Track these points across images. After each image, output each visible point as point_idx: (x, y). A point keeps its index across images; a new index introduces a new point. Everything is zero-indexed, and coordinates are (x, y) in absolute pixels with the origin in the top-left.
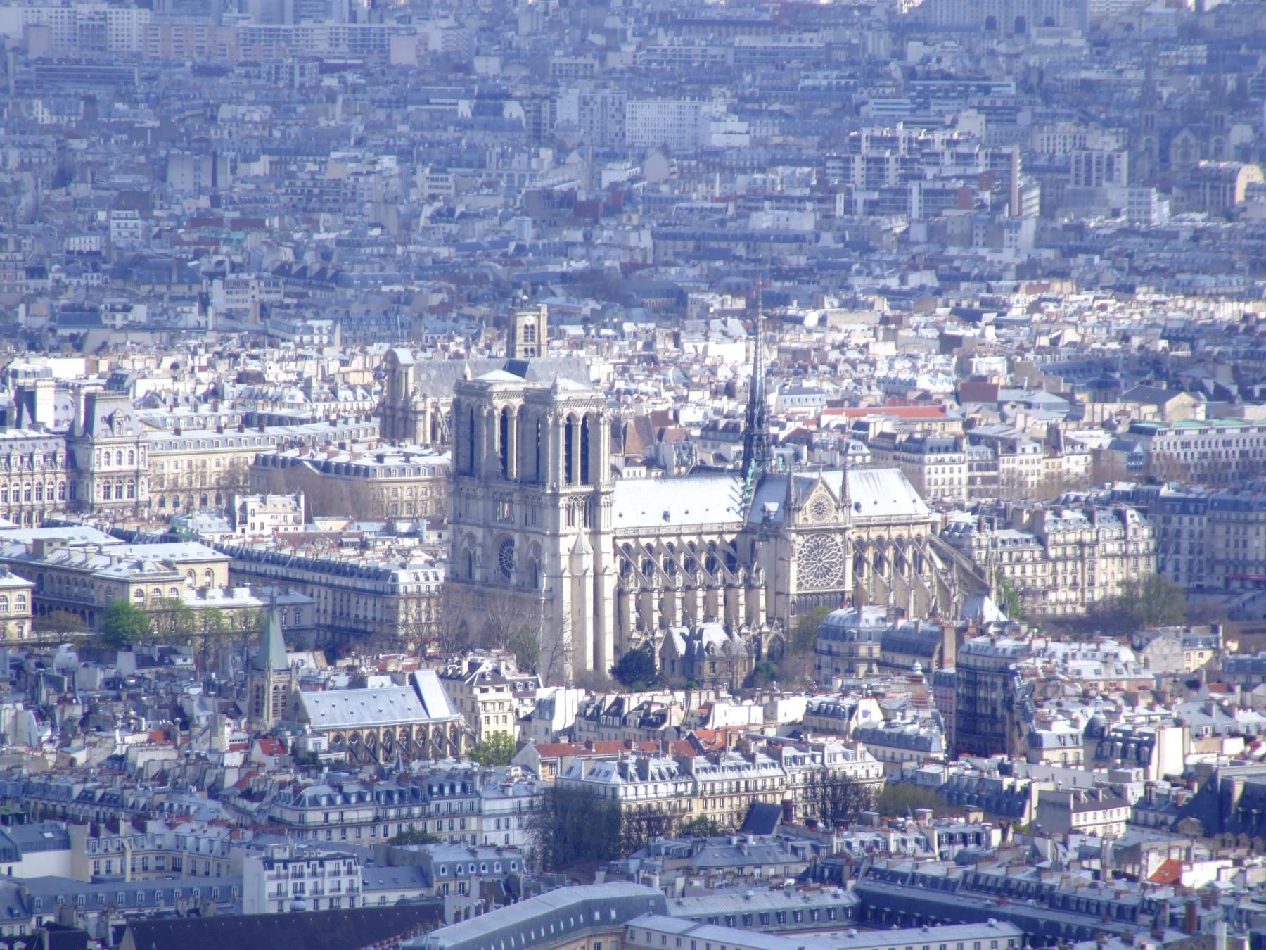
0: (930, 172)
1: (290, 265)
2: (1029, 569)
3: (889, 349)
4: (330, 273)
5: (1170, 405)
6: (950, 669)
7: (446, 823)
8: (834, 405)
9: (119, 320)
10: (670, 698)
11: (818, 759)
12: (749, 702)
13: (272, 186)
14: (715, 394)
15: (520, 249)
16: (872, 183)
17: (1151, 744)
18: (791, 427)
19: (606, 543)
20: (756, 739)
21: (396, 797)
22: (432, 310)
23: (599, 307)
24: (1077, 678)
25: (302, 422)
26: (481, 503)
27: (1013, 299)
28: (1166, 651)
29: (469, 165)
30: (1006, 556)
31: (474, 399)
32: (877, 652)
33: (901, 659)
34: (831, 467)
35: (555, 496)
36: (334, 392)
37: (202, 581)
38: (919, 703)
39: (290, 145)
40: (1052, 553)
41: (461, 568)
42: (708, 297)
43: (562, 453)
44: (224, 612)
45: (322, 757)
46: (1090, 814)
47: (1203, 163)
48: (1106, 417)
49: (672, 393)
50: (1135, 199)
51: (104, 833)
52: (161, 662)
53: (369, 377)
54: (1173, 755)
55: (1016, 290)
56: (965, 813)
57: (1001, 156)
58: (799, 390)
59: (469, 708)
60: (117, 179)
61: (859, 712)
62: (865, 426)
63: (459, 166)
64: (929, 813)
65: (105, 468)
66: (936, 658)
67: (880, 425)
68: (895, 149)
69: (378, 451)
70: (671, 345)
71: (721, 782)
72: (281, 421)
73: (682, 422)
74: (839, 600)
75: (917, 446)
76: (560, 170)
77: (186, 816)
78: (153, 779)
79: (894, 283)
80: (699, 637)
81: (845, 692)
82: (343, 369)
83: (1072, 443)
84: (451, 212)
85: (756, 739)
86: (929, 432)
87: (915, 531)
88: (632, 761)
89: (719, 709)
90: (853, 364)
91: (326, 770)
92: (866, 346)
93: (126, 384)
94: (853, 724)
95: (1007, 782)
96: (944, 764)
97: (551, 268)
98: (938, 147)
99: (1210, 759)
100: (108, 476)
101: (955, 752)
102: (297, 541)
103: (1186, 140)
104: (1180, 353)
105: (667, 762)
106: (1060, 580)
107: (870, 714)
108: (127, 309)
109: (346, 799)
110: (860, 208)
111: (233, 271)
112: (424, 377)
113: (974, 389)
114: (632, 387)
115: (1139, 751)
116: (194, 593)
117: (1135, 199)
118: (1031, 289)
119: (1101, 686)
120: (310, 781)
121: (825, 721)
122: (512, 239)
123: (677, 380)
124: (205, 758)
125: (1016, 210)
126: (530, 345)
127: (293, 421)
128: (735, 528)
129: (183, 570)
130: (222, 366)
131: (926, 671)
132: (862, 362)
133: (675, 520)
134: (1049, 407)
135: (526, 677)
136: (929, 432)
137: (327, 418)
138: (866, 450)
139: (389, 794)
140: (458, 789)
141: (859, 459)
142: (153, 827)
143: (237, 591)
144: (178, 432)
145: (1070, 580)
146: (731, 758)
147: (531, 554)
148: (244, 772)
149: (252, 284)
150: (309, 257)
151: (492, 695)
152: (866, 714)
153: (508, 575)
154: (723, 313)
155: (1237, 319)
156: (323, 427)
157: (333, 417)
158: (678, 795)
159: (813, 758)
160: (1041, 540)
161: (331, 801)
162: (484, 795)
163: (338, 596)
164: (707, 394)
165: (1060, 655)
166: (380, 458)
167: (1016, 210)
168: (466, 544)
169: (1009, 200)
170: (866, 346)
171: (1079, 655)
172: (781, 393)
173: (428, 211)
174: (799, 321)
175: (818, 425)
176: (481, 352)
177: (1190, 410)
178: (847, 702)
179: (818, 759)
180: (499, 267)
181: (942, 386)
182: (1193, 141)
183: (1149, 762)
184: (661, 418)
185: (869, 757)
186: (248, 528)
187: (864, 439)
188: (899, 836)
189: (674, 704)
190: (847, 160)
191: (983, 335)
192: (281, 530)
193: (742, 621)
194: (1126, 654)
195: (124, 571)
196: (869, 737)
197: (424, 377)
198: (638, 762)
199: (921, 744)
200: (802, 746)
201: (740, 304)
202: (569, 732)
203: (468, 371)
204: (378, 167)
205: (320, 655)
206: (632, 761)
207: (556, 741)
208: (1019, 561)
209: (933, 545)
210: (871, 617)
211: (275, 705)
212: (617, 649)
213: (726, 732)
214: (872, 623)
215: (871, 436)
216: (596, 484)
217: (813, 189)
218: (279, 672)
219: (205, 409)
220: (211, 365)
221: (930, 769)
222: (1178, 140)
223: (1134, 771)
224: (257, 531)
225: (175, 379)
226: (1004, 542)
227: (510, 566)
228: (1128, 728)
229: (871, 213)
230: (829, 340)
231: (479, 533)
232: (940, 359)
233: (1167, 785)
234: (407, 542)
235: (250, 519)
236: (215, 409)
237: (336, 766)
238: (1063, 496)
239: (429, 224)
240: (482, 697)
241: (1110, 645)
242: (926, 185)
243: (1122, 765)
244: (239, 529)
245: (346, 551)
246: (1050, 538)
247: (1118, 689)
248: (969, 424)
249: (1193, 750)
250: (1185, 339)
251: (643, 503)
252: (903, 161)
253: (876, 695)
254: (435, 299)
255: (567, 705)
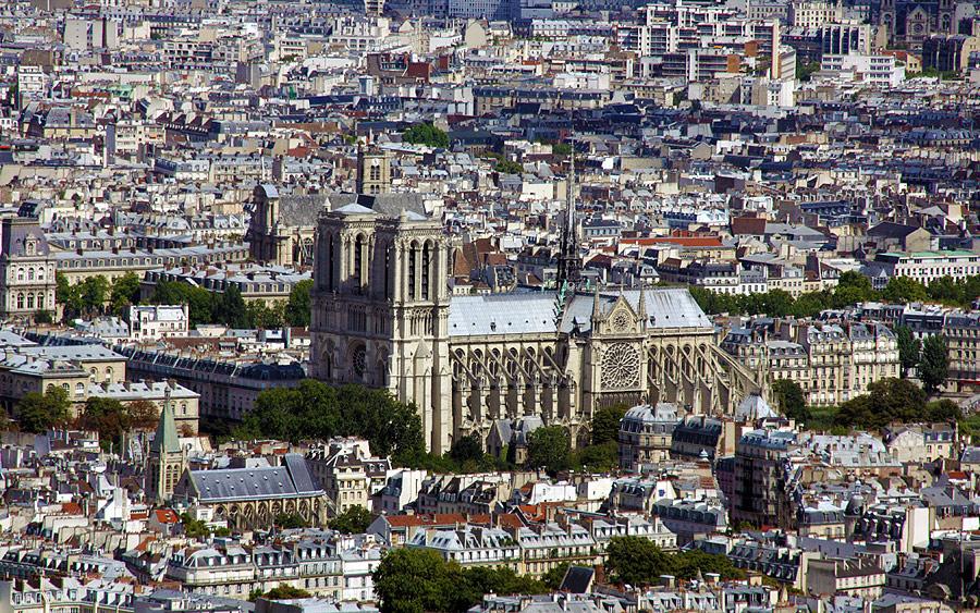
0: (705, 40)
1: (171, 114)
2: (794, 373)
3: (673, 189)
4: (205, 120)
5: (909, 238)
6: (730, 455)
7: (312, 581)
8: (628, 236)
9: (28, 157)
10: (498, 479)
11: (623, 531)
12: (565, 482)
13: (153, 47)
14: (529, 225)
15: (364, 102)
16: (658, 46)
17: (902, 521)
18: (593, 253)
19: (443, 348)
20: (571, 513)
21: (271, 559)
22: (291, 152)
23: (430, 152)
24: (839, 465)
25: (185, 245)
26: (338, 314)
27: (776, 148)
28: (911, 443)
29: (318, 31)
30: (774, 362)
31: (333, 228)
32: (669, 440)
33: (689, 448)
34: (628, 287)
35: (401, 309)
36: (211, 219)
37: (102, 377)
38: (706, 484)
39: (168, 13)
40: (814, 360)
41: (321, 368)
42: (521, 144)
43: (407, 274)
44: (123, 403)
45: (208, 524)
46: (851, 580)
47: (933, 35)
48: (856, 247)
49: (495, 225)
50: (878, 64)
51: (27, 587)
52: (71, 445)
53: (239, 208)
54: (920, 529)
55: (778, 140)
56: (748, 578)
57: (765, 28)
58: (599, 223)
59: (330, 486)
60: (21, 40)
61: (656, 492)
62: (655, 253)
63: (309, 31)
64: (716, 577)
65: (18, 282)
66: (718, 447)
67: (667, 253)
68: (675, 23)
69: (249, 271)
70: (491, 183)
71: (542, 549)
72: (167, 244)
73: (502, 249)
74: (635, 397)
75: (697, 270)
76: (394, 38)
77: (94, 571)
78: (66, 542)
79: (675, 134)
80: (521, 428)
81: (645, 476)
82: (217, 201)
83: (827, 268)
84: (305, 71)
85: (571, 513)
86: (708, 258)
87: (700, 341)
88: (468, 530)
89: (538, 488)
90: (645, 199)
91: (213, 535)
92: (654, 186)
93: (35, 212)
94: (652, 501)
95: (782, 551)
96: (728, 534)
97: (389, 118)
98: (711, 21)
99: (952, 535)
100: (21, 288)
101: (736, 526)
102: (181, 344)
103: (919, 16)
104: (917, 195)
105: (499, 531)
106: (819, 384)
107: (665, 492)
108: (34, 149)
109: (230, 559)
110: (646, 71)
111: (123, 118)
112: (287, 208)
113: (746, 223)
114: (461, 219)
115: (893, 529)
116: (99, 388)
117: (878, 64)
118: (790, 140)
119: (858, 472)
120: (199, 544)
121: (631, 499)
122: (357, 94)
123: (498, 213)
124: (110, 525)
125: (775, 75)
126: (375, 182)
127: (177, 244)
128: (553, 337)
129: (87, 367)
130: (116, 197)
131: (711, 457)
132: (650, 199)
133: (501, 328)
134: (807, 238)
135: (377, 459)
136: (708, 258)
137: (205, 242)
138: (655, 273)
139: (266, 556)
140: (323, 553)
141: (650, 280)
142: (69, 582)
143: (133, 386)
144: (80, 252)
145: (828, 385)
146: (550, 529)
147: (380, 358)
148: (144, 537)
149: (139, 129)
150: (187, 107)
151: (349, 474)
152: (662, 493)
153: (360, 374)
154: (534, 158)
155: (965, 165)
156: (203, 250)
157: (211, 241)
158: (507, 560)
159: (619, 529)
160: (806, 350)
161: (218, 560)
162: (344, 558)
163: (217, 391)
164: (523, 226)
165: (823, 446)
166: (250, 276)
167: (775, 75)
168: (325, 349)
169: (771, 65)
170: (654, 186)
171: (839, 447)
172: (584, 225)
173: (285, 69)
174: (599, 164)
175: (616, 252)
176: (333, 188)
177: (927, 243)
178: (646, 483)
179: (623, 531)
180: (346, 118)
181: (719, 220)
182: (924, 17)
183: (901, 537)
184: (484, 244)
185: (665, 529)
186: (141, 334)
187: (654, 264)
188: (694, 595)
189: (502, 484)
190: (636, 31)
191: (751, 179)
192: (169, 335)
193: (555, 415)
194: (878, 445)
195: (40, 367)
196: (662, 512)
197: (287, 208)
198: (473, 531)
199: (708, 520)
200: (610, 520)
201: (548, 150)
202: (413, 505)
203: (328, 204)
204: (243, 33)
205: (205, 440)
206: (468, 530)
207: (404, 513)
208: (784, 367)
209: (714, 353)
210: (666, 413)
211: (168, 482)
212: (453, 437)
213: (545, 505)
214: (666, 418)
215: (660, 262)
216: (436, 300)
217: (607, 55)
218: (172, 453)
219: (102, 233)
220: (106, 197)
221: (715, 540)
222: (911, 16)
223: (889, 544)
224: (149, 336)
225: (77, 208)
226: (773, 351)
227: (362, 367)
228: (883, 507)
229: (654, 76)
230: (623, 182)
231: (337, 340)
232: (717, 197)
233: (916, 556)
234: (274, 346)
235: (143, 326)
236: (110, 232)
237: (220, 532)
238: (822, 313)
239: (286, 81)
240: (340, 476)
241: (866, 438)
242: (700, 53)
243: (877, 539)
244: (133, 334)
245: (224, 353)
246: (812, 348)
247: (873, 475)
248: (740, 252)
249: (937, 527)
250: (921, 183)
251: (471, 316)
252: (682, 32)
253: (670, 478)
254: (294, 144)
255: (413, 482)
